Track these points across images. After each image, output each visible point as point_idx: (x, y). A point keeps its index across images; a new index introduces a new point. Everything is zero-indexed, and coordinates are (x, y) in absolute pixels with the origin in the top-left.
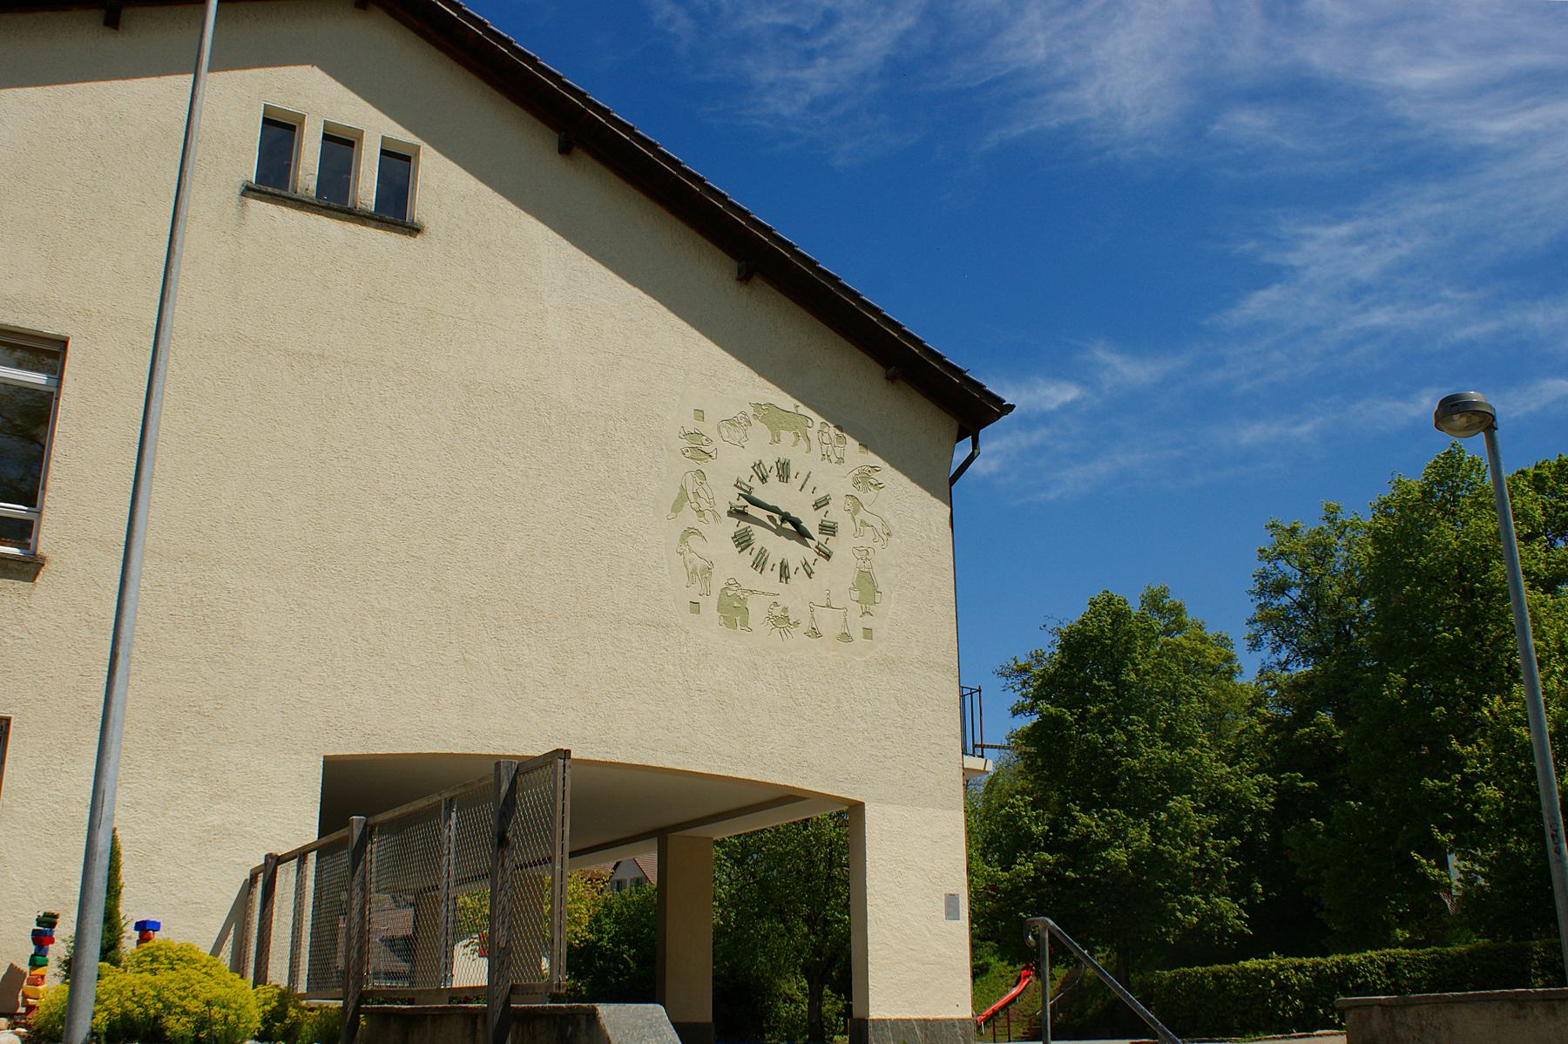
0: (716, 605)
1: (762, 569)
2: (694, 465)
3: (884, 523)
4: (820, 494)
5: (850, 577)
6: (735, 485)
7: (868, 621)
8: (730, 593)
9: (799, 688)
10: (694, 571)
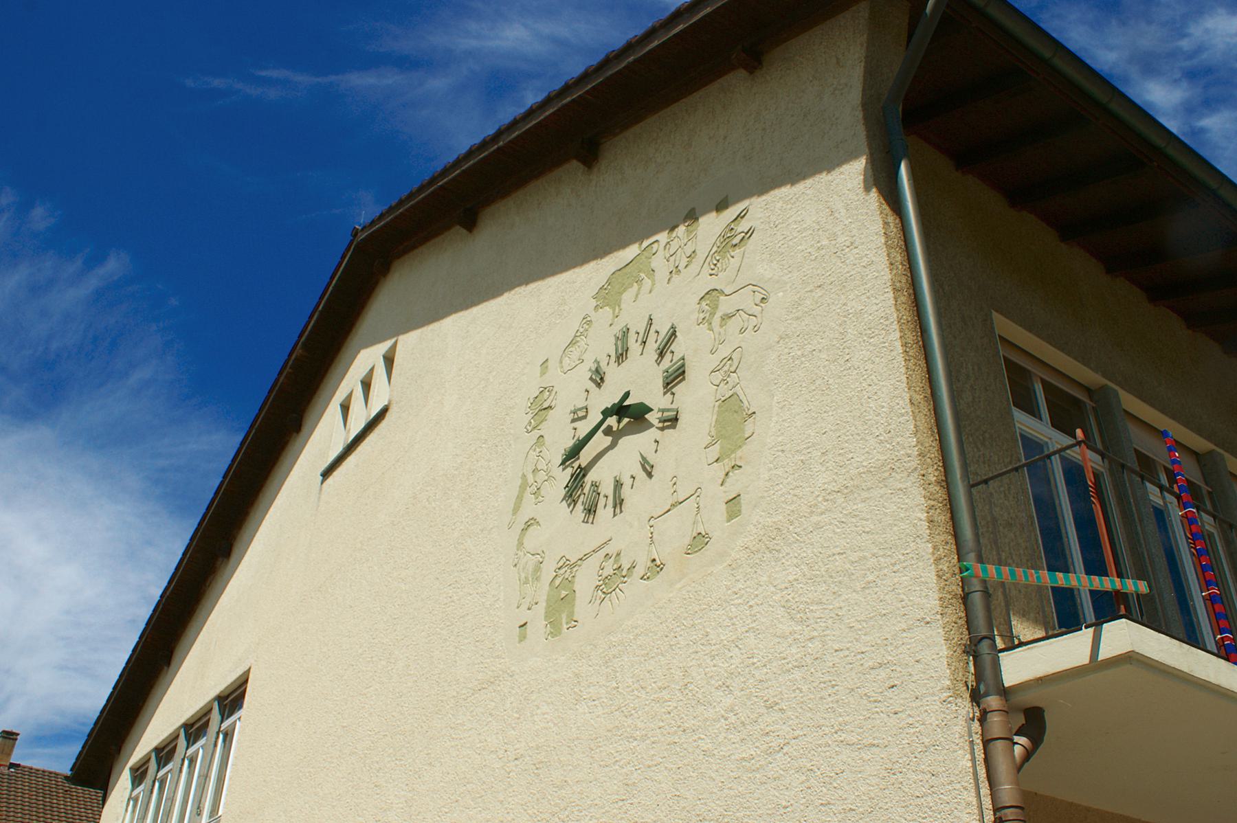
4: (664, 331)
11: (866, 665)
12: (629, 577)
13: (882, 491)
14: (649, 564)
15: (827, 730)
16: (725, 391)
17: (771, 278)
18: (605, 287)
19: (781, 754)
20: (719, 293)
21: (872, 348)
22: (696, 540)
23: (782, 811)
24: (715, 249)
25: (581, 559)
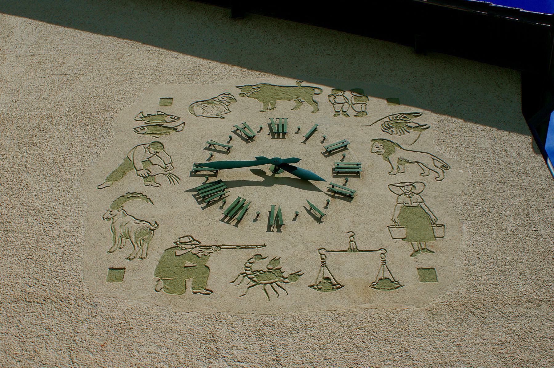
1: (239, 221)
2: (150, 139)
3: (434, 157)
7: (425, 260)
8: (179, 252)
10: (126, 235)
14: (321, 279)
22: (383, 281)
24: (387, 120)
25: (217, 246)
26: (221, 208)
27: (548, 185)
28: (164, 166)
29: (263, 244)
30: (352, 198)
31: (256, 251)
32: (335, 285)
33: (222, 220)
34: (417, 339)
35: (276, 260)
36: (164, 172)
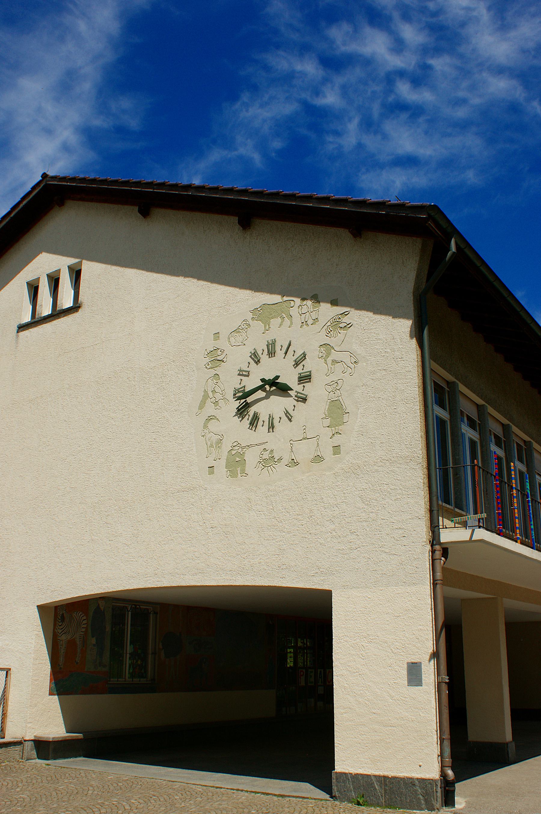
0: (225, 464)
2: (213, 372)
4: (299, 353)
5: (323, 407)
6: (239, 375)
9: (281, 508)
10: (212, 446)
11: (394, 527)
12: (278, 463)
13: (406, 467)
14: (290, 461)
15: (376, 546)
16: (334, 397)
17: (360, 354)
18: (259, 309)
19: (356, 550)
20: (331, 347)
21: (407, 408)
22: (316, 457)
23: (356, 570)
24: (329, 324)
25: (248, 446)
26: (248, 419)
27: (412, 367)
28: (221, 393)
29: (266, 442)
30: (306, 400)
31: (264, 446)
32: (296, 463)
33: (249, 428)
34: (327, 491)
35: (272, 451)
36: (222, 398)
